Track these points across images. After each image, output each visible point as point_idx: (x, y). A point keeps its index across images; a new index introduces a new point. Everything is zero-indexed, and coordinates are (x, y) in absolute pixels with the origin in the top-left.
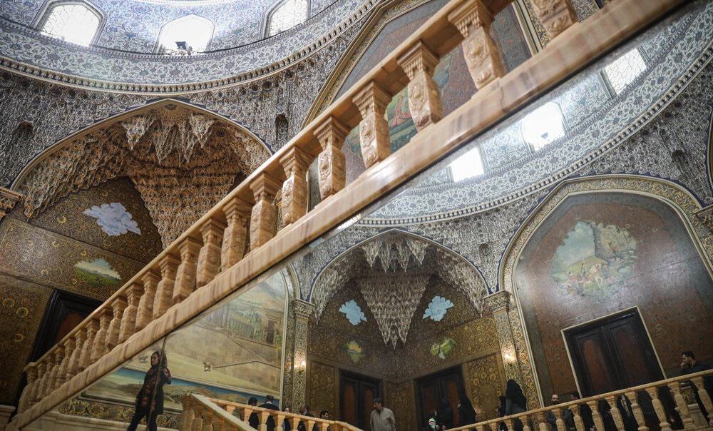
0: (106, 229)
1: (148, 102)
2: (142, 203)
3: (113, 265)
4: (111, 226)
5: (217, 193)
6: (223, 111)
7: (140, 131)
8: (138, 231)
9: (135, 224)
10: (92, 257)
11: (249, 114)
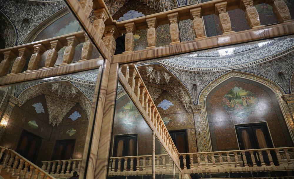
0: (37, 111)
1: (62, 80)
2: (46, 103)
3: (37, 123)
4: (38, 110)
5: (69, 106)
6: (82, 90)
7: (56, 87)
8: (44, 112)
9: (43, 110)
10: (32, 120)
11: (89, 94)
